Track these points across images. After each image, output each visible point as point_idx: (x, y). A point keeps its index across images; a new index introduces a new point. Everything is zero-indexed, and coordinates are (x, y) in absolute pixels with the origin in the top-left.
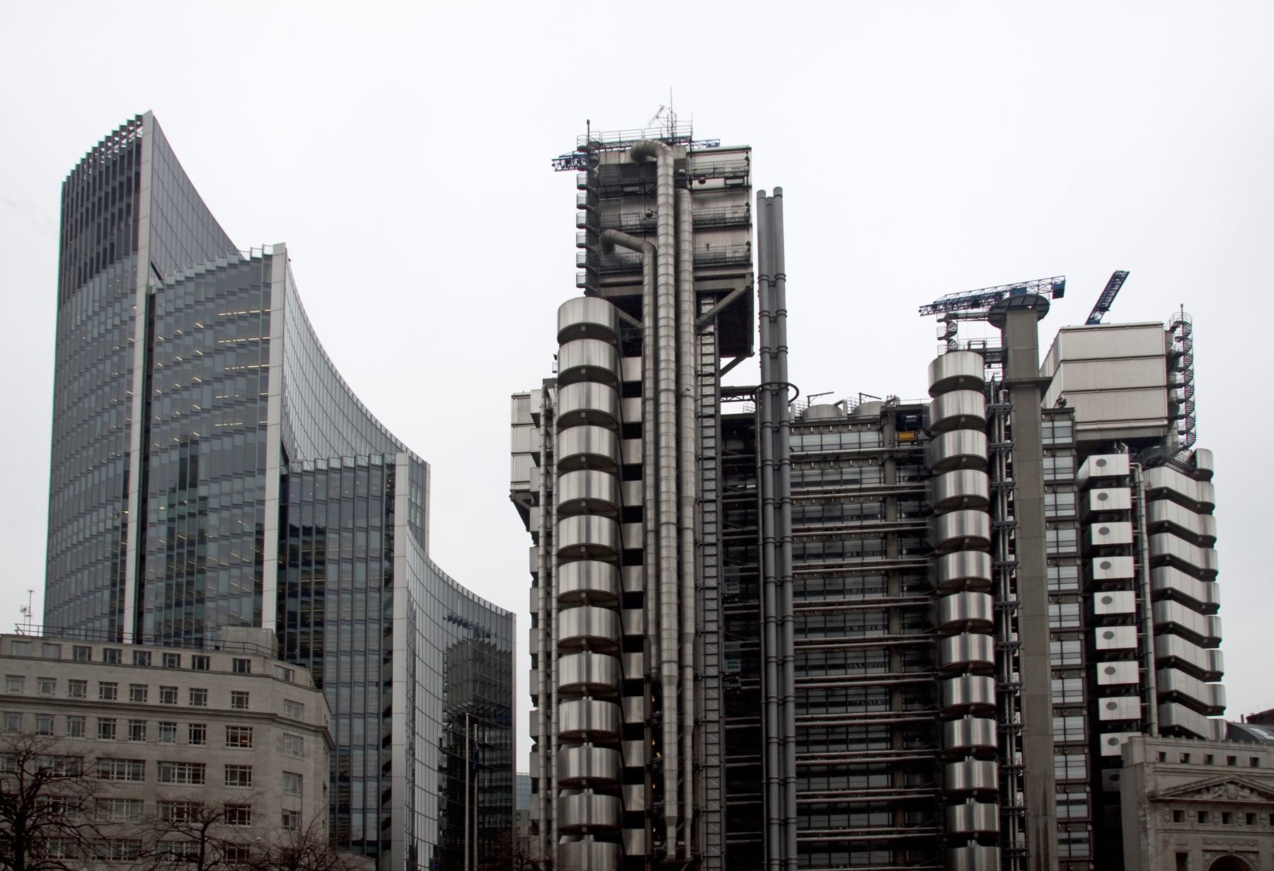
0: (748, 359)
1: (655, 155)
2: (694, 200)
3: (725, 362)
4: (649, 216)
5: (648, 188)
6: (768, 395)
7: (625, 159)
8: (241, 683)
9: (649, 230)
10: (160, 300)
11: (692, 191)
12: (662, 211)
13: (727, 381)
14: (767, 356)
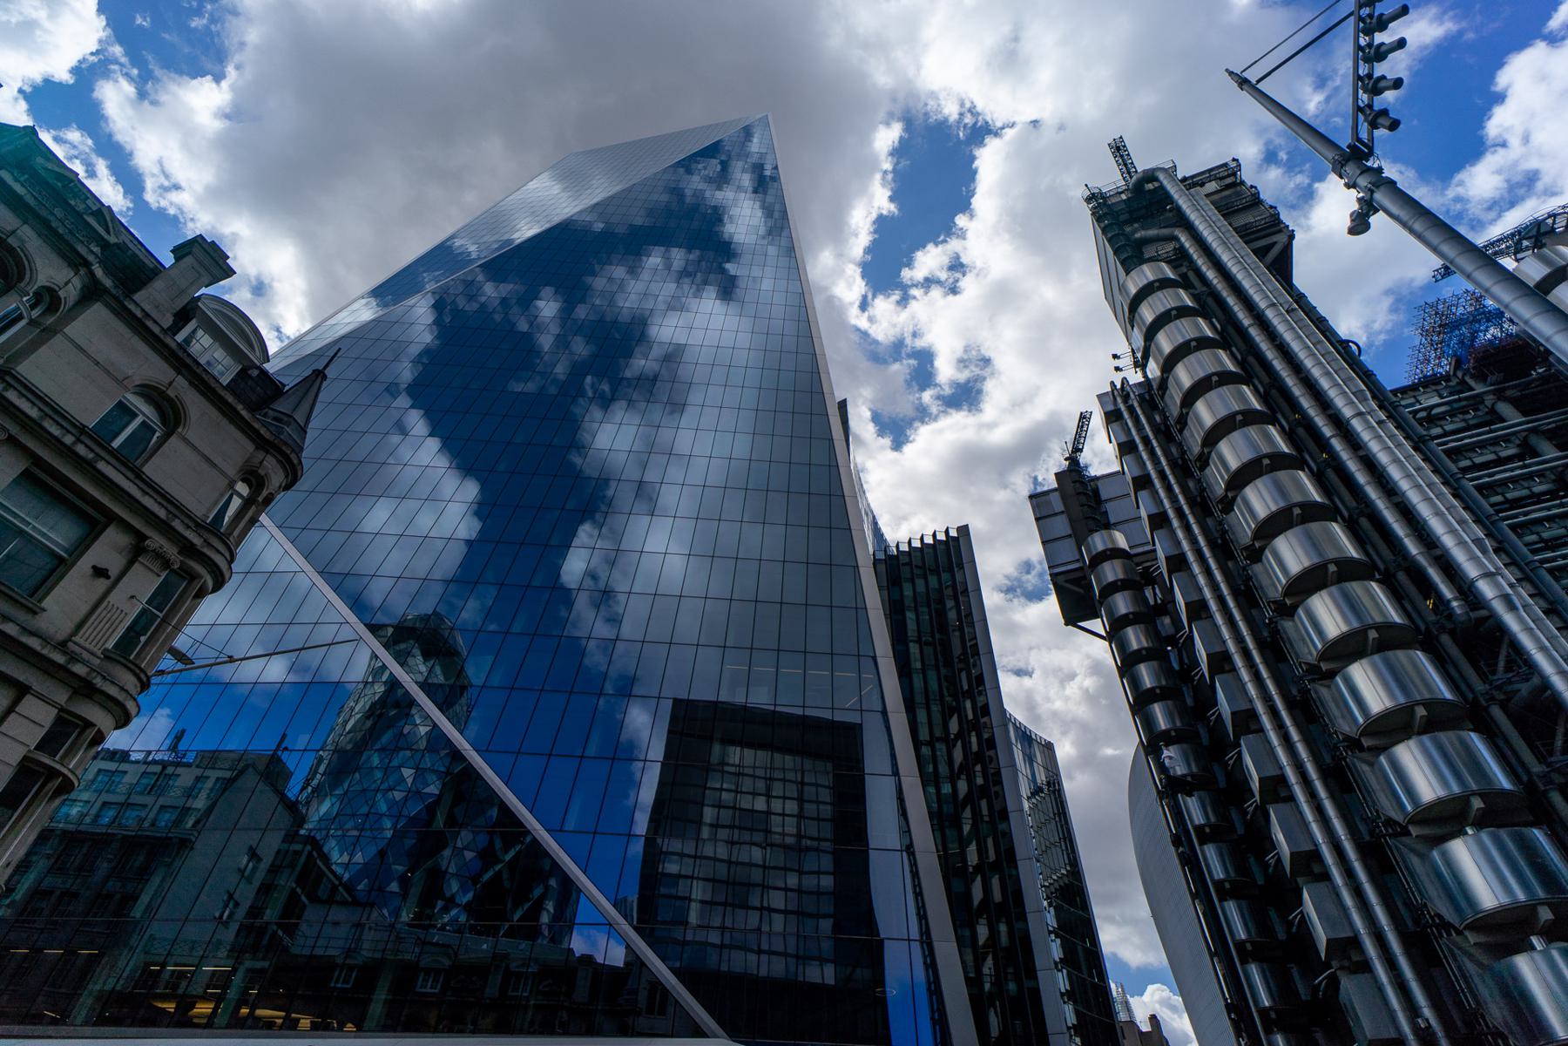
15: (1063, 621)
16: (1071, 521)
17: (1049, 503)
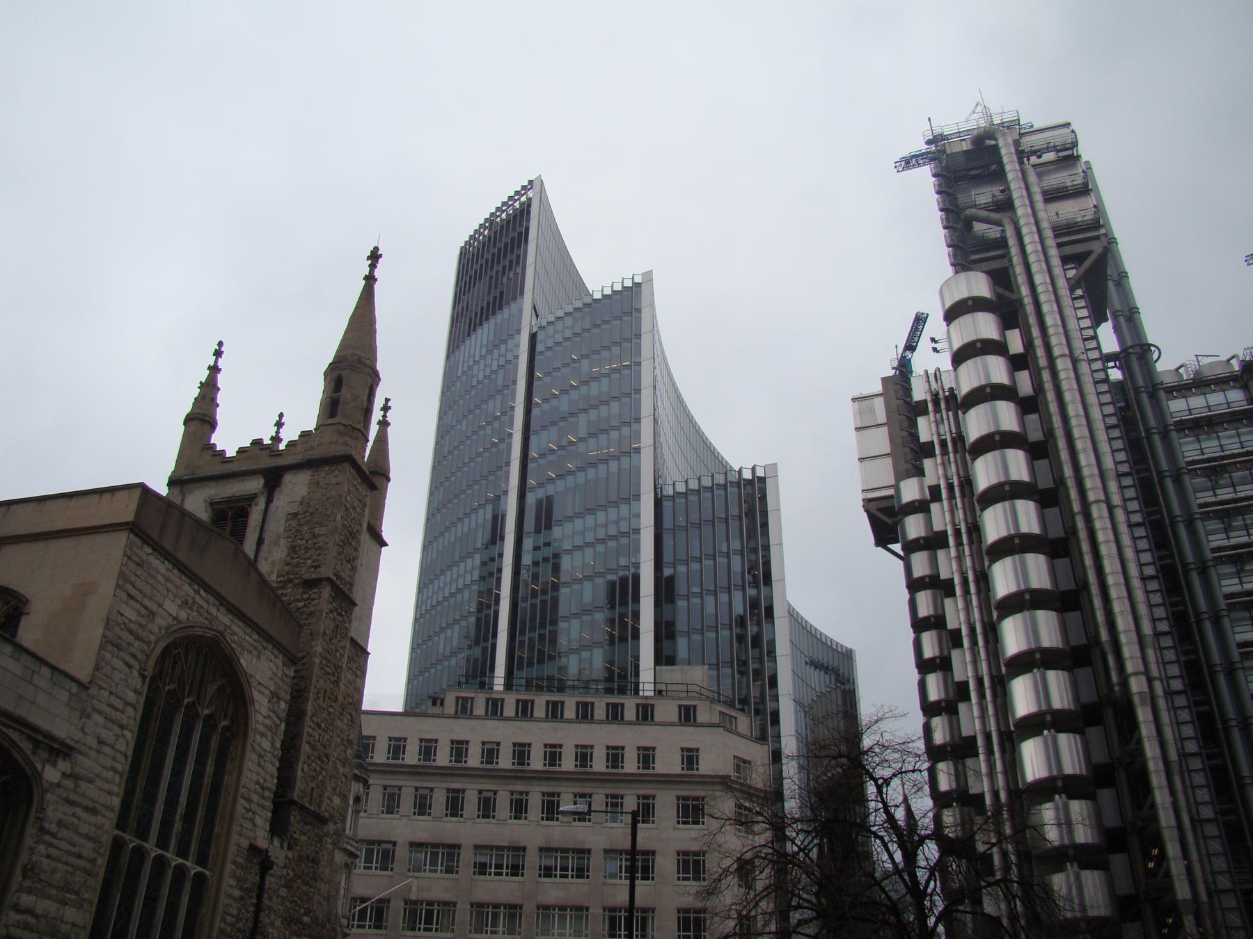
0: (1104, 324)
1: (993, 138)
2: (1039, 175)
4: (1002, 191)
6: (1134, 359)
7: (966, 146)
8: (690, 737)
10: (540, 337)
12: (1013, 186)
14: (1122, 319)
15: (874, 542)
16: (892, 441)
17: (872, 411)
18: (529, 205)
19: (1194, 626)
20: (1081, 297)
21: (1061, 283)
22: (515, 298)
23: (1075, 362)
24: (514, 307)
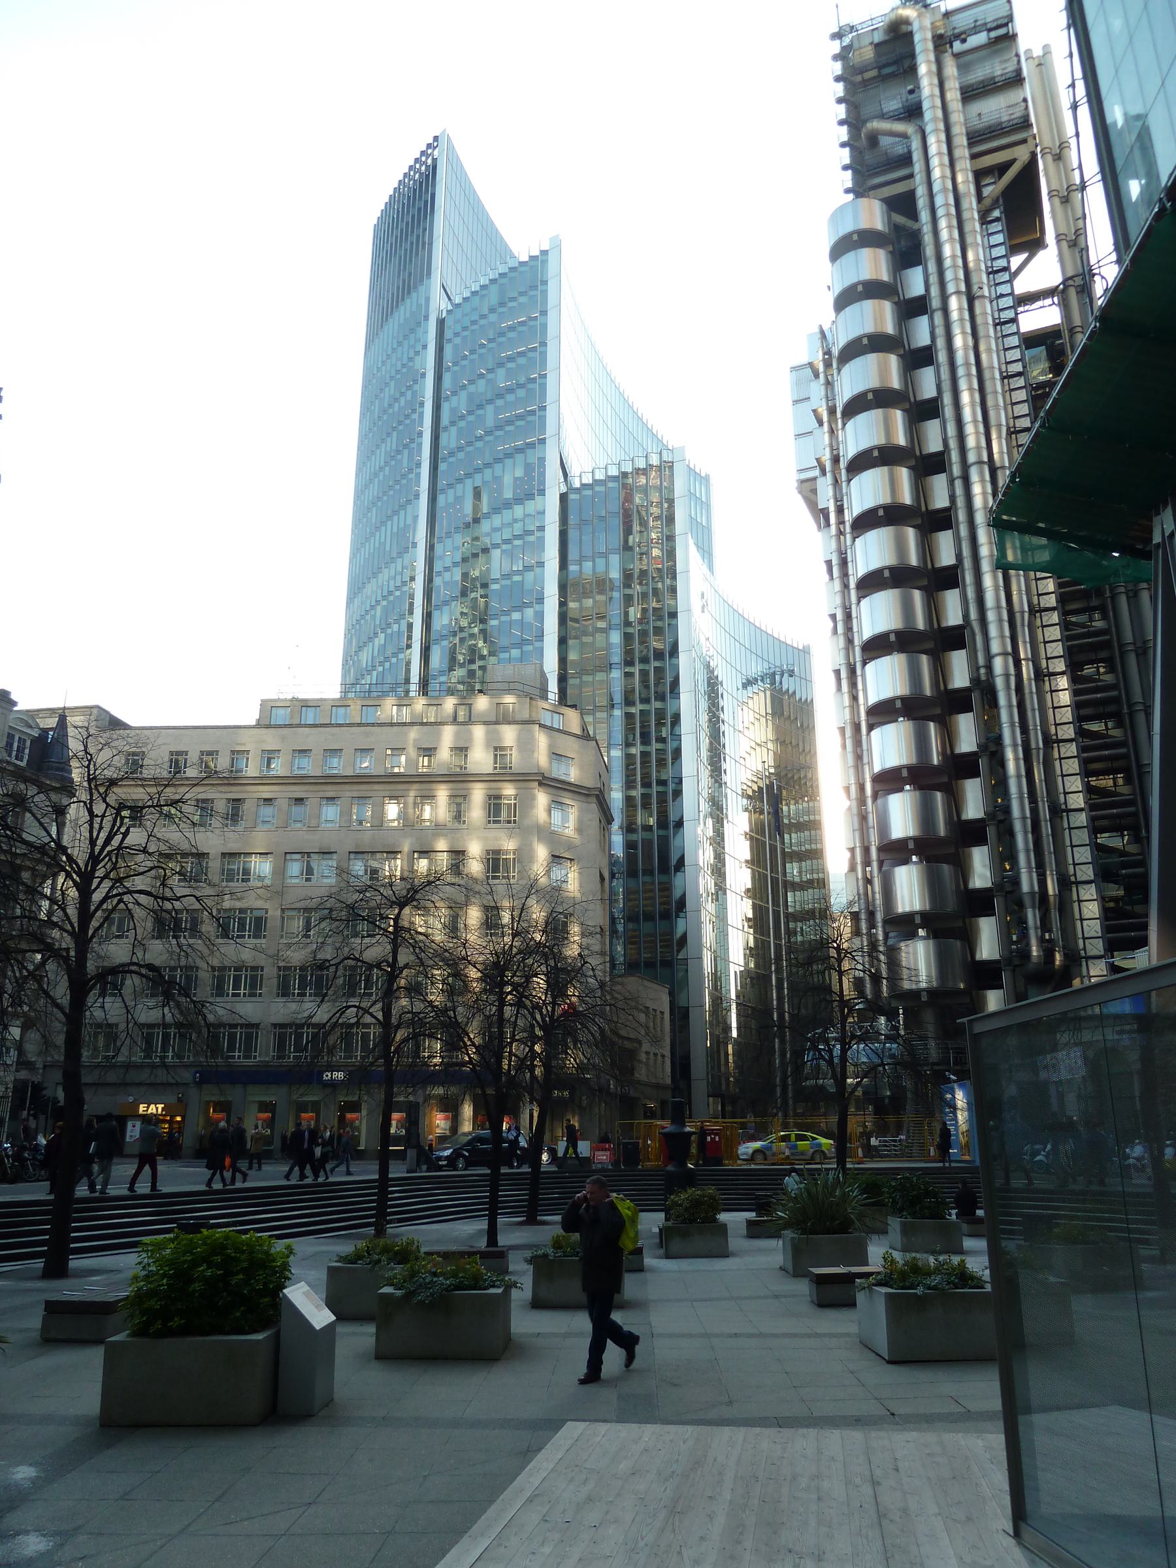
2: (963, 68)
3: (1016, 261)
4: (911, 92)
5: (906, 64)
6: (1072, 292)
9: (913, 112)
10: (448, 323)
11: (956, 56)
13: (1022, 285)
14: (1064, 244)
18: (435, 168)
19: (1109, 600)
20: (997, 220)
21: (971, 205)
22: (422, 280)
23: (971, 300)
24: (422, 289)
